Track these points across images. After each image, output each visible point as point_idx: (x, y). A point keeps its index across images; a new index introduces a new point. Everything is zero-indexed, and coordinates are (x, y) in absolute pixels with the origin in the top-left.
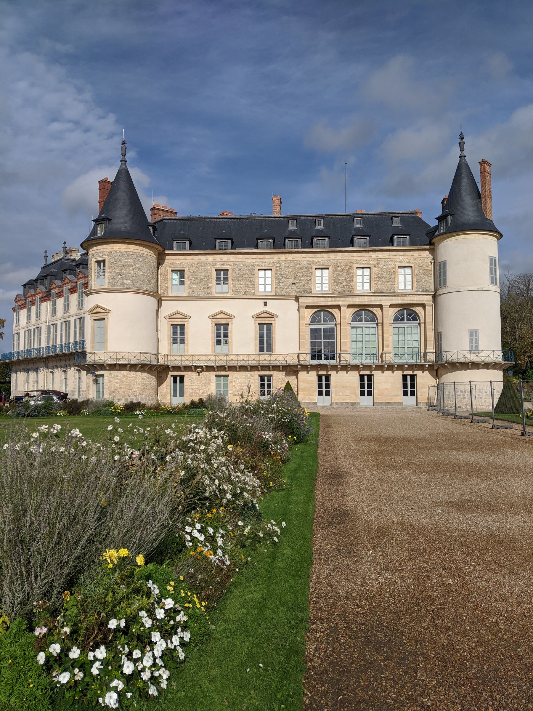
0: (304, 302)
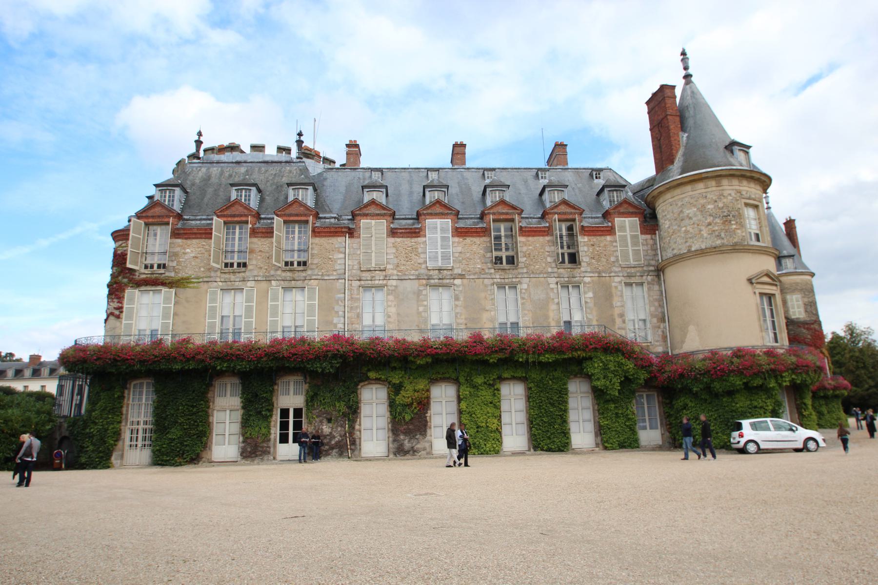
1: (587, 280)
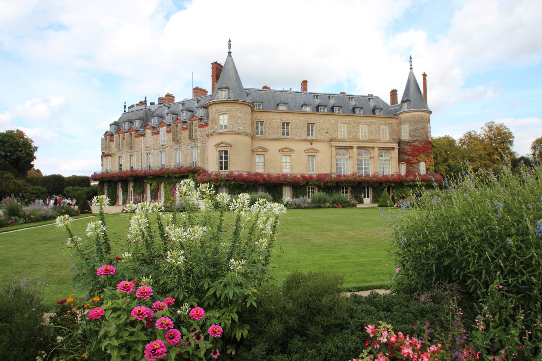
1: (199, 145)
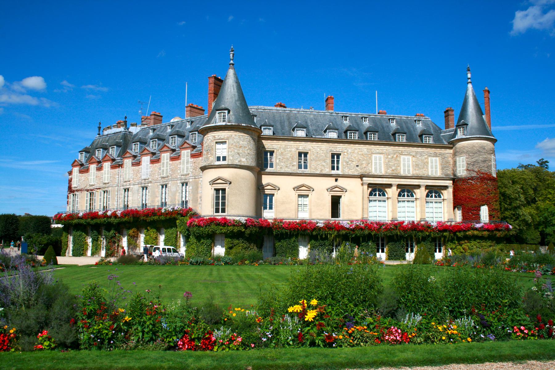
0: (367, 180)
1: (191, 180)
